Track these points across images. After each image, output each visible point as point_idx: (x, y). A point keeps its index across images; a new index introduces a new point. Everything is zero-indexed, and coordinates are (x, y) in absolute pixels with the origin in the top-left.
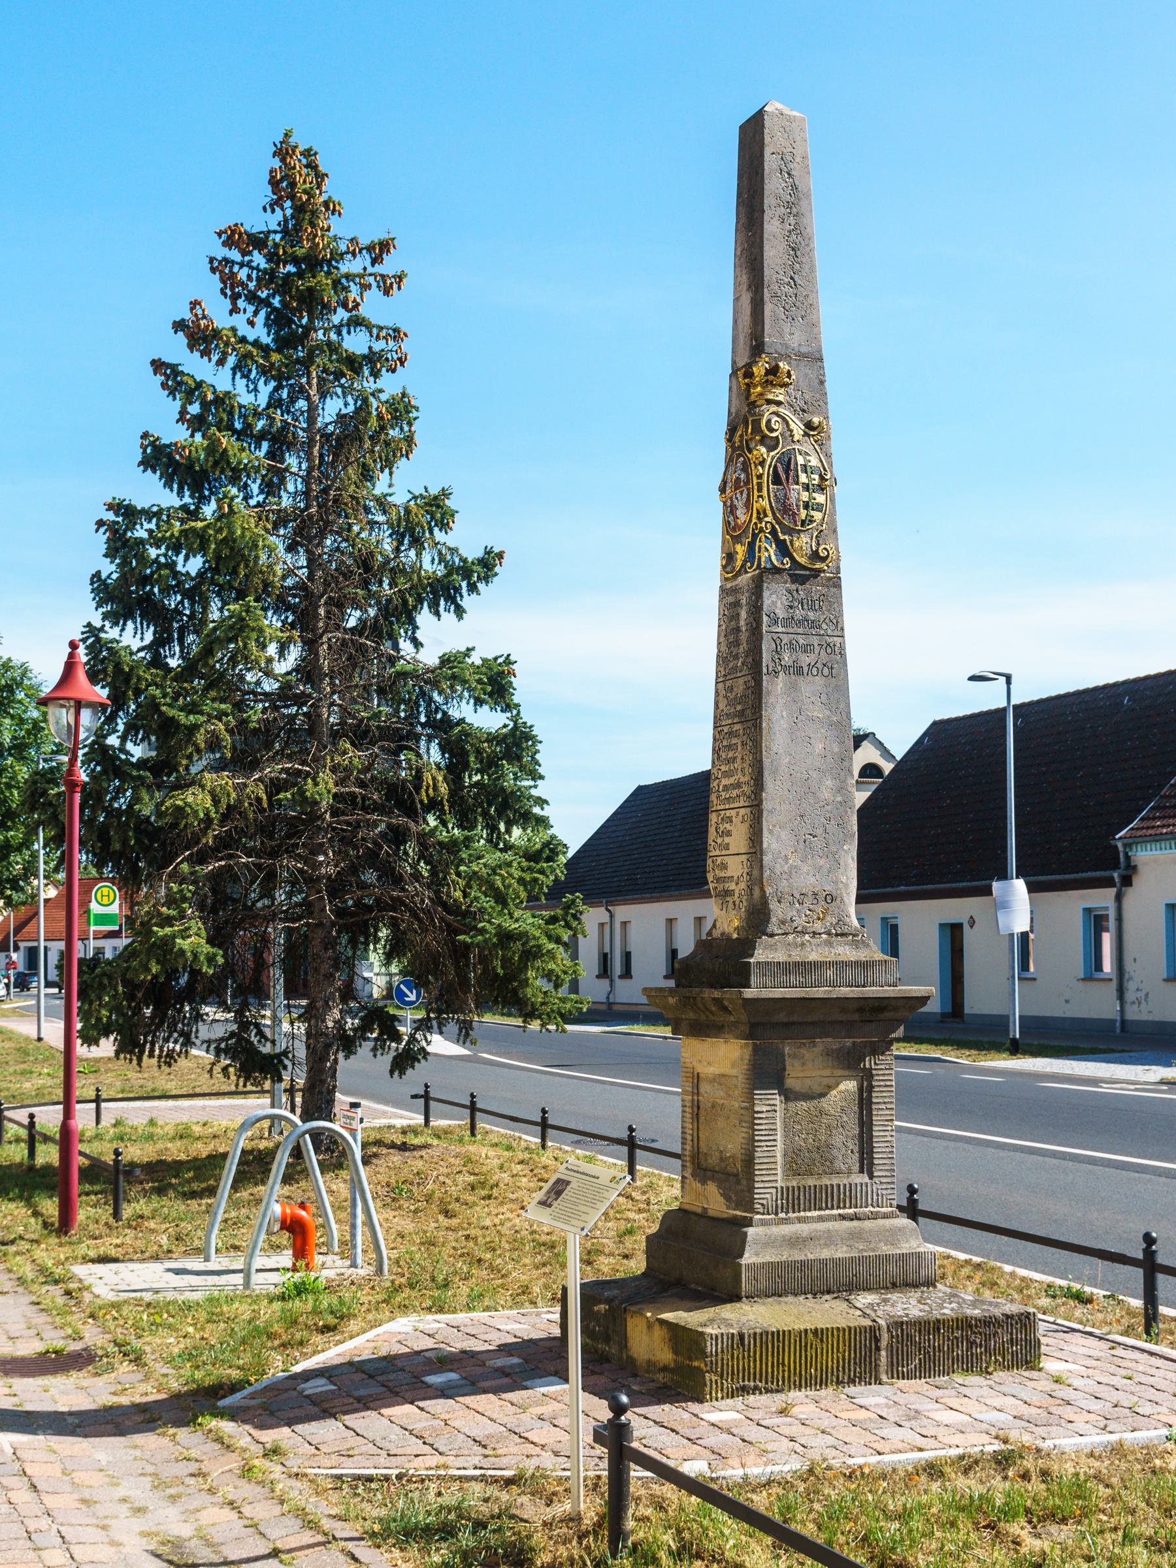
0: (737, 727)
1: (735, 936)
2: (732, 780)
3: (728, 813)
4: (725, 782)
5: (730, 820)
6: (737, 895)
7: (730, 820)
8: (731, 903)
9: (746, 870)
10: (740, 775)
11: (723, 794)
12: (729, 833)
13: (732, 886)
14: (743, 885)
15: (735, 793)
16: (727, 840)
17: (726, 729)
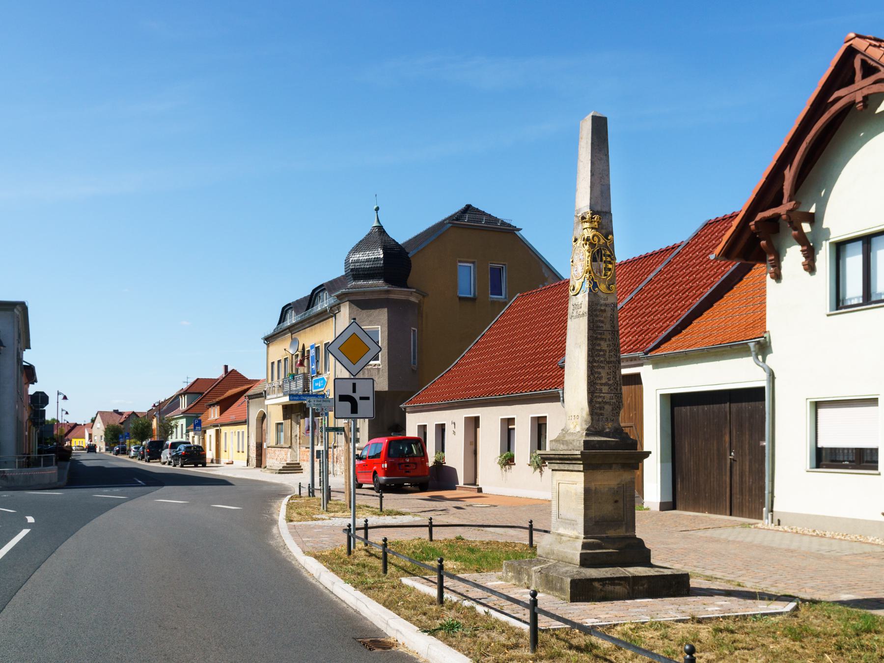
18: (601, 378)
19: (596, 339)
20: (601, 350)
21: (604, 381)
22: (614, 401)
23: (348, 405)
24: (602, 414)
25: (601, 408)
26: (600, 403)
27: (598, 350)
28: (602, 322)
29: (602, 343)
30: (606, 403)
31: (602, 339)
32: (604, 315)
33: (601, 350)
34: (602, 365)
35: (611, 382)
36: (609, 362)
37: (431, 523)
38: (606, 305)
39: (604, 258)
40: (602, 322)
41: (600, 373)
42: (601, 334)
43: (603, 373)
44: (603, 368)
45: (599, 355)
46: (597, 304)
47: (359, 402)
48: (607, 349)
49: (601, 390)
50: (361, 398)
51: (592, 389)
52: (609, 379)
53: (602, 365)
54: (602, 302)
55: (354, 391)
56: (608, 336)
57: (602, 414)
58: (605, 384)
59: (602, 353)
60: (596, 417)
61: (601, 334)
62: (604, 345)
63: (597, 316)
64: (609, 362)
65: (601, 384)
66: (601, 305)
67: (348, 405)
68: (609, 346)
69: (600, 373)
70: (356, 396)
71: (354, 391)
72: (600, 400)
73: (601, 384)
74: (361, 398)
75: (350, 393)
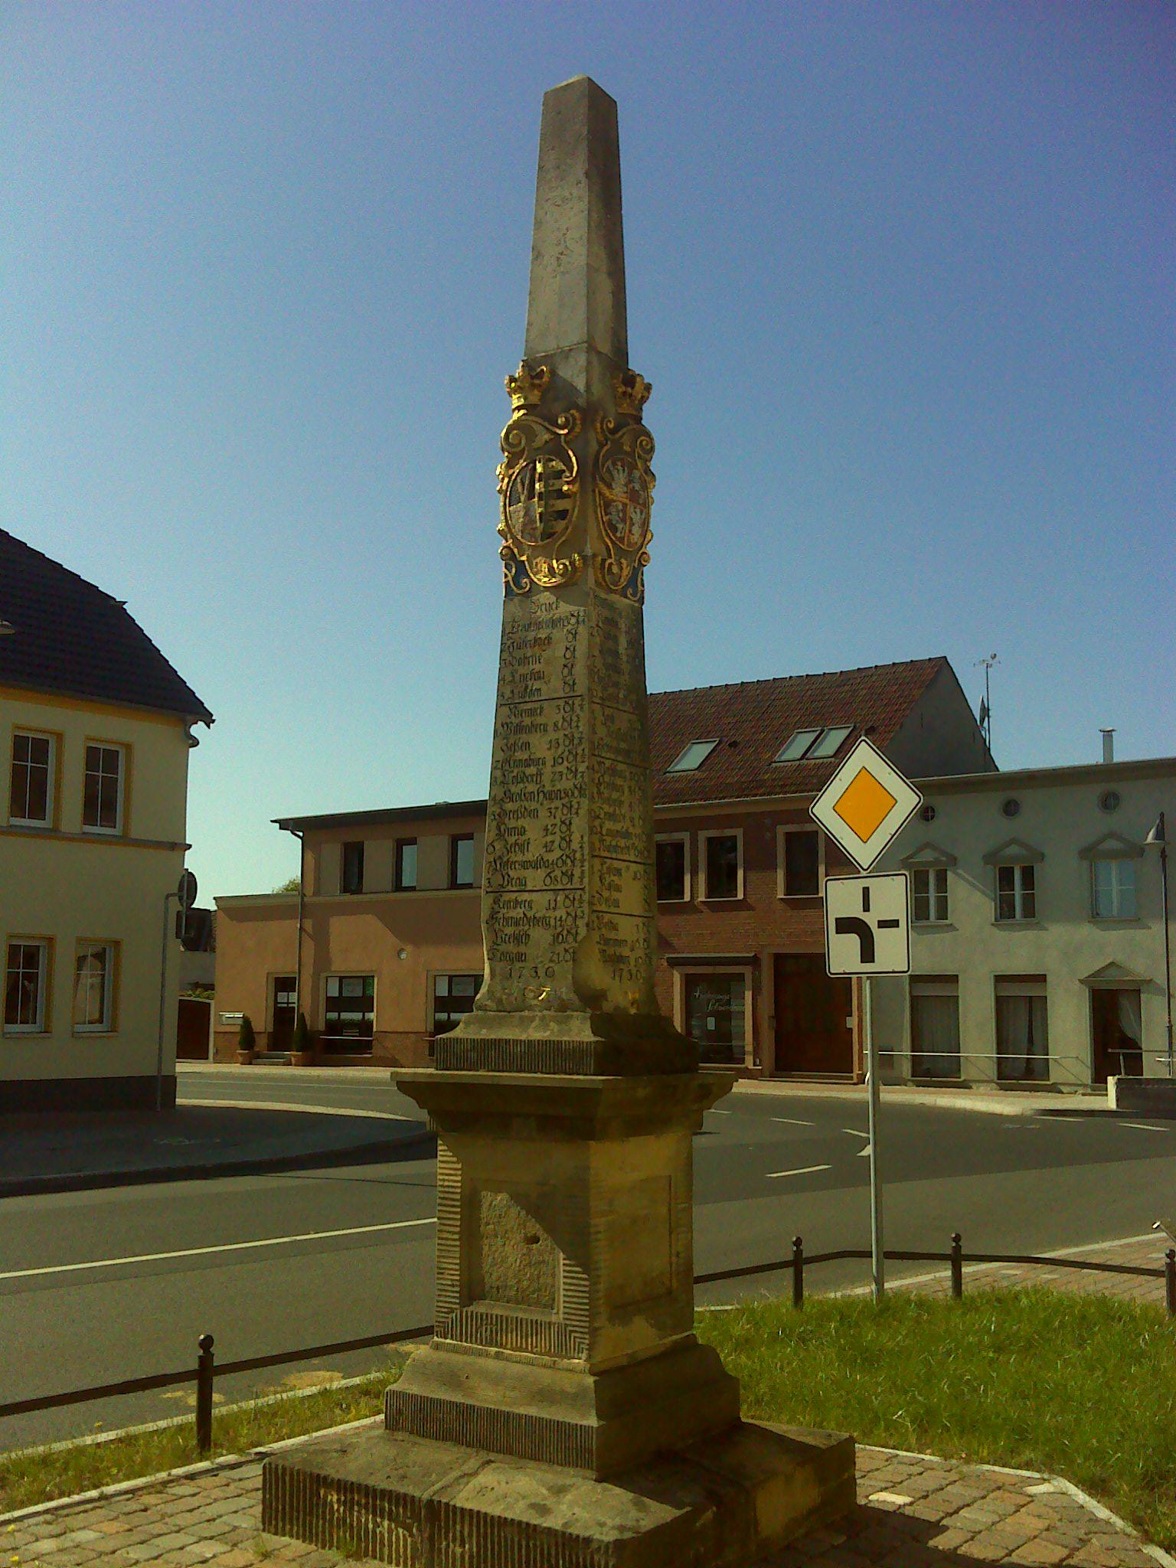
0: (621, 767)
1: (633, 1011)
2: (618, 827)
3: (616, 864)
5: (618, 872)
6: (632, 963)
7: (618, 872)
8: (624, 973)
9: (642, 936)
10: (628, 823)
11: (608, 839)
12: (618, 889)
13: (626, 952)
14: (640, 953)
15: (622, 843)
16: (616, 895)
17: (608, 763)
18: (523, 847)
19: (520, 729)
20: (528, 763)
22: (561, 913)
23: (853, 940)
24: (521, 957)
27: (520, 763)
28: (538, 676)
30: (536, 921)
31: (534, 728)
33: (528, 763)
34: (533, 805)
35: (551, 857)
36: (550, 796)
37: (957, 1249)
38: (554, 623)
40: (538, 676)
41: (522, 831)
42: (532, 712)
43: (533, 831)
44: (534, 814)
45: (523, 778)
46: (527, 627)
48: (549, 756)
49: (522, 882)
50: (883, 924)
51: (497, 880)
53: (533, 805)
54: (543, 615)
55: (866, 909)
56: (552, 715)
58: (535, 865)
61: (532, 712)
62: (540, 746)
63: (524, 661)
64: (550, 796)
65: (525, 865)
66: (539, 625)
67: (853, 940)
69: (522, 831)
70: (871, 919)
71: (866, 909)
72: (517, 913)
73: (525, 865)
74: (883, 924)
75: (856, 912)
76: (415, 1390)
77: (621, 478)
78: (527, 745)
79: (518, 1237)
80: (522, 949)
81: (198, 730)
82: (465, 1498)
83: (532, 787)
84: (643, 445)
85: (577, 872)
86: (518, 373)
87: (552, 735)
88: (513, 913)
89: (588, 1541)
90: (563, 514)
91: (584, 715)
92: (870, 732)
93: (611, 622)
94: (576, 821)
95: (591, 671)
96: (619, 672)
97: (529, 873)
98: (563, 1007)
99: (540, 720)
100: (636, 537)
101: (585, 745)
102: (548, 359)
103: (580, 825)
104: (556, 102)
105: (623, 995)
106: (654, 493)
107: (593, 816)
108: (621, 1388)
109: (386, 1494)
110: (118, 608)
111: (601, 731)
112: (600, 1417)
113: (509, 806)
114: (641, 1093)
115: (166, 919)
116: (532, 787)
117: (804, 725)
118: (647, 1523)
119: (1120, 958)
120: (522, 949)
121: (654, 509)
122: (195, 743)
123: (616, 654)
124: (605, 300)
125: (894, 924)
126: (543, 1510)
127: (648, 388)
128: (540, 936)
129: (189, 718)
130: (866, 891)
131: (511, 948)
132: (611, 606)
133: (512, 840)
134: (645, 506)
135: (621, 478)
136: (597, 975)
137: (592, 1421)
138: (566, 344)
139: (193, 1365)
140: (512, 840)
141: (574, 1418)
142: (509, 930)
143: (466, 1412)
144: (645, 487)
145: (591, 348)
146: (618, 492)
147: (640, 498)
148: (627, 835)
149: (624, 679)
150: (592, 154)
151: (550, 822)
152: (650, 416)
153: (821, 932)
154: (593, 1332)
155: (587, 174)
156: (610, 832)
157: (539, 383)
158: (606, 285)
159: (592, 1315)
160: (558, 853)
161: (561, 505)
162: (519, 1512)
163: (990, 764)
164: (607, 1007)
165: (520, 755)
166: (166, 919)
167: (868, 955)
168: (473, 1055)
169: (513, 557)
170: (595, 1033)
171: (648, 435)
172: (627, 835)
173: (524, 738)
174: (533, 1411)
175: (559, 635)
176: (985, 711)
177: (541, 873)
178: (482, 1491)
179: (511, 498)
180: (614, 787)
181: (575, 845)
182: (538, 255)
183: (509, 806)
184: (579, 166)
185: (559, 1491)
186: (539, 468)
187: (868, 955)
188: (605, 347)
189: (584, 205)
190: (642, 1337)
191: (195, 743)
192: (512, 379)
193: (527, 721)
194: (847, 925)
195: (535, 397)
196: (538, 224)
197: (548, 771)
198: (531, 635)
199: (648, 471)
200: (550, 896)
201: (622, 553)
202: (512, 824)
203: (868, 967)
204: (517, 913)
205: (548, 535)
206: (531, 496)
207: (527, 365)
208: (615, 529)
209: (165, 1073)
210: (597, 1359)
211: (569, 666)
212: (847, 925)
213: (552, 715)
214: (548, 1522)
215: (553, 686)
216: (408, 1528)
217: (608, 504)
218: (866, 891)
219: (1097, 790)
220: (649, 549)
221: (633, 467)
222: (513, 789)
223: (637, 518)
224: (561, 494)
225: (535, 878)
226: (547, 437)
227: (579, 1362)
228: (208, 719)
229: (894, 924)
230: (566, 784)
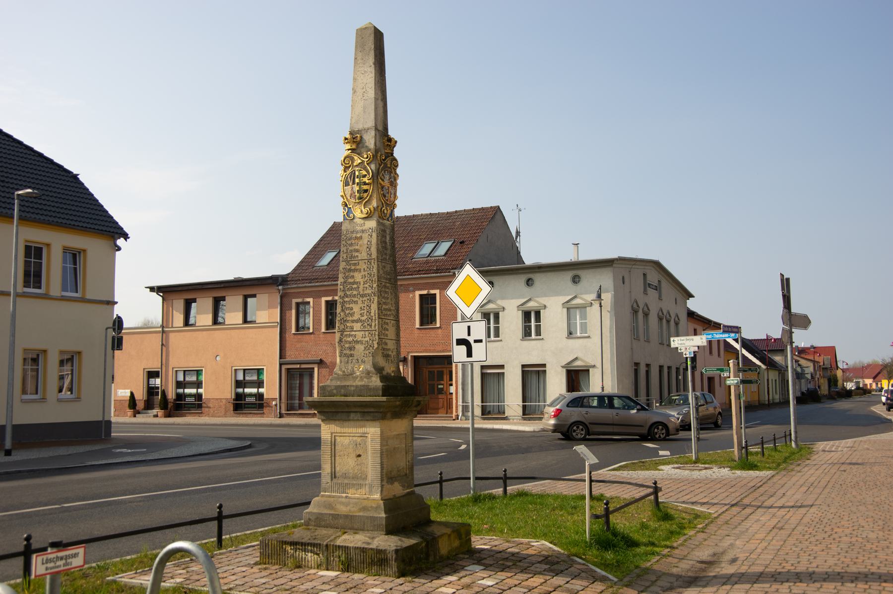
2: (387, 307)
4: (384, 306)
5: (387, 324)
7: (387, 324)
12: (387, 330)
13: (390, 353)
14: (395, 353)
18: (352, 315)
19: (350, 270)
20: (354, 283)
21: (356, 317)
22: (367, 339)
23: (463, 348)
24: (351, 355)
25: (350, 349)
26: (350, 343)
27: (351, 283)
28: (357, 251)
29: (356, 274)
30: (357, 342)
31: (355, 270)
32: (360, 243)
33: (354, 283)
34: (355, 299)
35: (363, 318)
36: (362, 296)
38: (363, 231)
39: (357, 180)
40: (357, 251)
41: (352, 309)
43: (356, 309)
44: (356, 302)
45: (352, 289)
46: (352, 232)
47: (474, 345)
48: (362, 281)
49: (352, 328)
50: (476, 341)
52: (362, 315)
53: (355, 299)
54: (359, 228)
55: (469, 335)
56: (363, 266)
57: (351, 355)
58: (357, 321)
59: (355, 286)
60: (345, 359)
64: (362, 296)
65: (353, 321)
67: (463, 348)
68: (364, 277)
70: (471, 339)
71: (469, 335)
72: (350, 339)
73: (353, 321)
74: (476, 341)
75: (465, 336)
76: (315, 511)
77: (387, 177)
78: (353, 277)
79: (353, 455)
80: (352, 352)
81: (120, 242)
82: (339, 542)
83: (355, 292)
84: (394, 163)
85: (373, 324)
86: (348, 136)
87: (363, 273)
88: (349, 339)
89: (385, 550)
90: (366, 191)
91: (375, 266)
92: (470, 260)
93: (384, 231)
94: (373, 305)
95: (378, 250)
96: (386, 249)
97: (354, 324)
98: (368, 373)
99: (358, 267)
100: (392, 199)
101: (376, 277)
102: (359, 131)
103: (374, 307)
104: (361, 32)
105: (389, 369)
106: (398, 181)
107: (379, 303)
108: (391, 505)
109: (308, 544)
110: (75, 177)
111: (381, 272)
112: (386, 513)
113: (346, 299)
114: (398, 403)
115: (106, 340)
116: (355, 292)
117: (429, 239)
118: (405, 545)
119: (580, 355)
120: (352, 352)
121: (398, 187)
122: (119, 249)
123: (386, 243)
124: (381, 110)
125: (481, 341)
126: (369, 544)
127: (396, 142)
128: (360, 348)
129: (116, 236)
130: (469, 327)
131: (348, 352)
132: (383, 225)
133: (347, 312)
134: (396, 187)
135: (387, 177)
136: (381, 362)
137: (384, 515)
138: (366, 126)
139: (216, 515)
140: (347, 312)
141: (376, 515)
142: (347, 346)
143: (336, 517)
144: (395, 180)
145: (376, 129)
146: (386, 183)
147: (393, 184)
148: (390, 310)
149: (388, 252)
150: (376, 56)
151: (362, 305)
152: (396, 153)
153: (451, 344)
154: (382, 486)
155: (374, 64)
156: (385, 309)
157: (355, 141)
158: (381, 104)
159: (382, 481)
160: (365, 317)
161: (365, 187)
162: (359, 545)
163: (520, 260)
164: (385, 373)
165: (350, 280)
166: (106, 340)
167: (469, 354)
168: (335, 391)
169: (346, 205)
170: (381, 381)
171: (395, 159)
172: (390, 310)
173: (352, 274)
174: (361, 514)
175: (365, 236)
176: (518, 233)
177: (359, 324)
178: (345, 540)
179: (346, 184)
180: (386, 292)
181: (372, 314)
182: (354, 91)
183: (346, 299)
184: (371, 60)
185: (373, 538)
186: (357, 173)
187: (469, 354)
188: (380, 128)
189: (373, 75)
190: (397, 489)
191: (119, 249)
192: (346, 139)
193: (353, 268)
194: (460, 342)
195: (354, 147)
196: (355, 79)
197: (361, 286)
198: (354, 235)
199: (396, 173)
200: (363, 333)
201: (387, 205)
202: (348, 306)
203: (470, 359)
204: (350, 339)
205: (360, 198)
206: (354, 183)
207: (351, 133)
208: (385, 196)
209: (106, 419)
210: (385, 493)
211: (369, 248)
212: (460, 342)
213: (363, 266)
214: (371, 547)
215: (364, 255)
216: (318, 554)
217: (383, 187)
218: (469, 327)
219: (569, 275)
220: (396, 202)
221: (391, 172)
222: (348, 293)
223: (393, 192)
224: (365, 184)
225: (357, 326)
226: (360, 161)
227: (377, 496)
228: (126, 236)
229: (481, 341)
230: (369, 291)
